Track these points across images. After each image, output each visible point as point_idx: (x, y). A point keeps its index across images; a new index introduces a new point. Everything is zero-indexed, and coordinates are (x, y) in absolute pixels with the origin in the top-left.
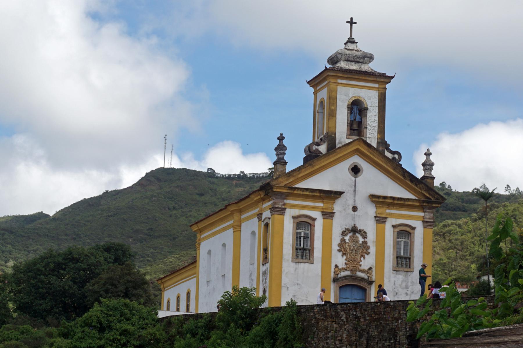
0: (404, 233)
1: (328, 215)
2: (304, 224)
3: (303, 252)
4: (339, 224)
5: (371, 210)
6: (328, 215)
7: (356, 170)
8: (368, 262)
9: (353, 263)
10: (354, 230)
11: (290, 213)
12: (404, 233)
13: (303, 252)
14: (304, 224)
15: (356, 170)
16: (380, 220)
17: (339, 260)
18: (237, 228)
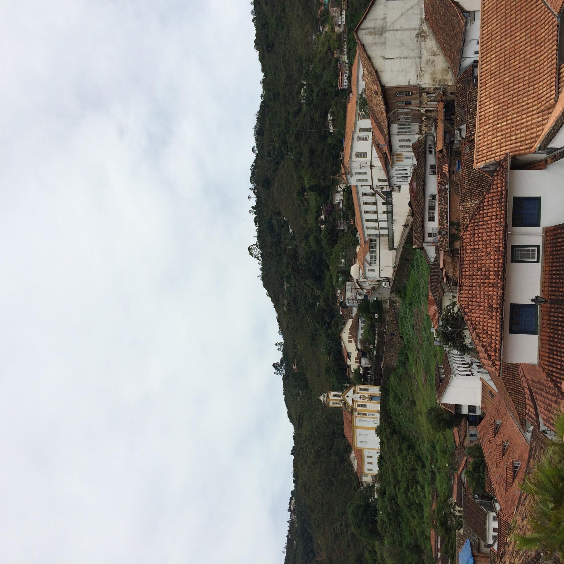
0: (361, 389)
1: (357, 401)
2: (359, 405)
3: (365, 406)
4: (359, 400)
5: (356, 395)
6: (357, 401)
7: (348, 397)
8: (367, 396)
9: (367, 398)
10: (360, 397)
11: (356, 407)
12: (361, 389)
13: (365, 406)
14: (359, 405)
15: (348, 397)
16: (358, 393)
17: (366, 400)
18: (357, 428)
